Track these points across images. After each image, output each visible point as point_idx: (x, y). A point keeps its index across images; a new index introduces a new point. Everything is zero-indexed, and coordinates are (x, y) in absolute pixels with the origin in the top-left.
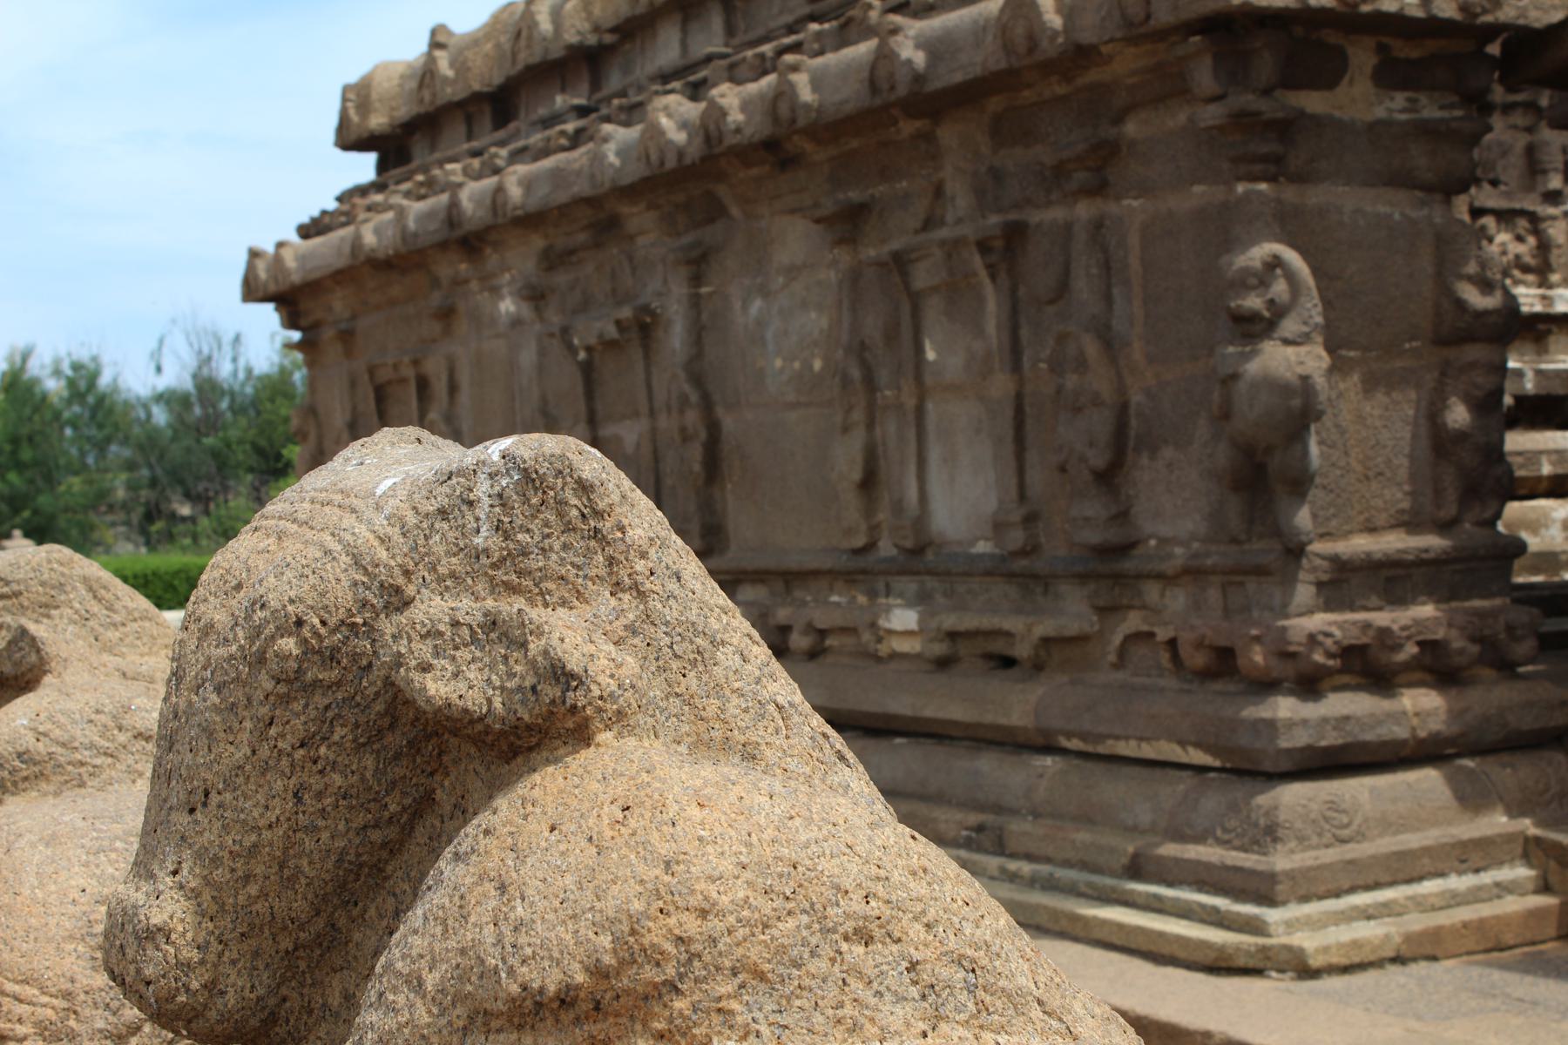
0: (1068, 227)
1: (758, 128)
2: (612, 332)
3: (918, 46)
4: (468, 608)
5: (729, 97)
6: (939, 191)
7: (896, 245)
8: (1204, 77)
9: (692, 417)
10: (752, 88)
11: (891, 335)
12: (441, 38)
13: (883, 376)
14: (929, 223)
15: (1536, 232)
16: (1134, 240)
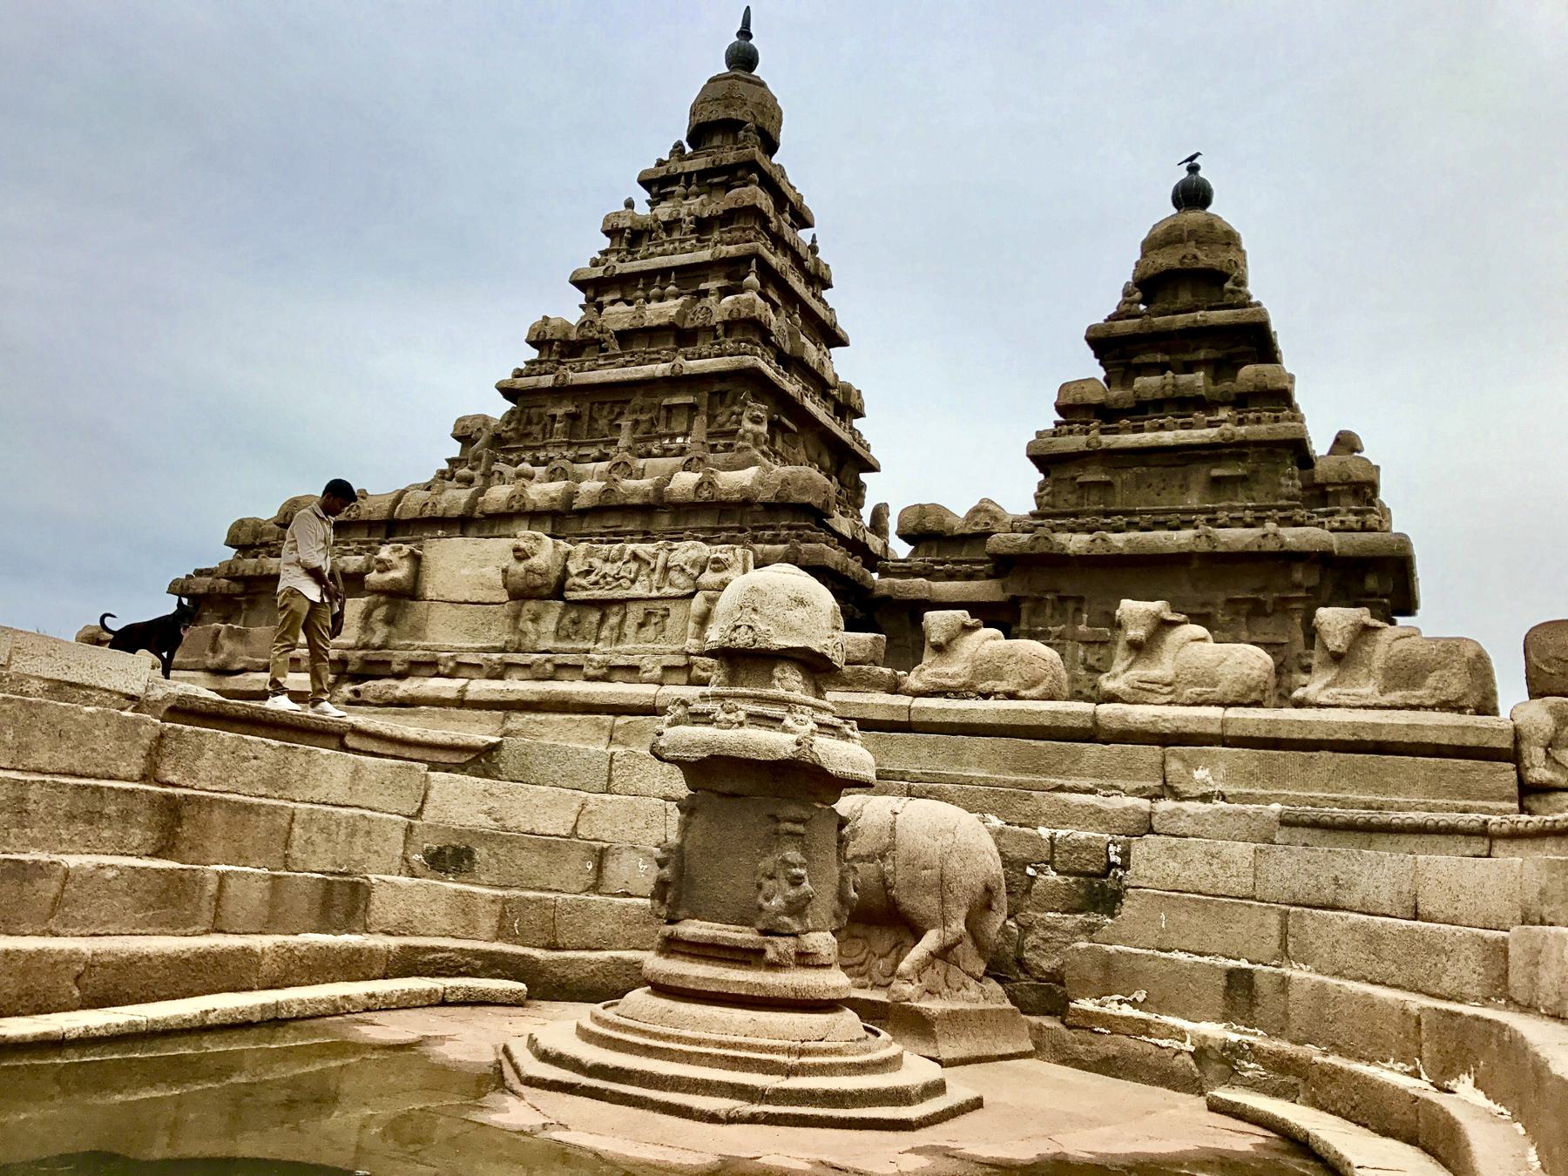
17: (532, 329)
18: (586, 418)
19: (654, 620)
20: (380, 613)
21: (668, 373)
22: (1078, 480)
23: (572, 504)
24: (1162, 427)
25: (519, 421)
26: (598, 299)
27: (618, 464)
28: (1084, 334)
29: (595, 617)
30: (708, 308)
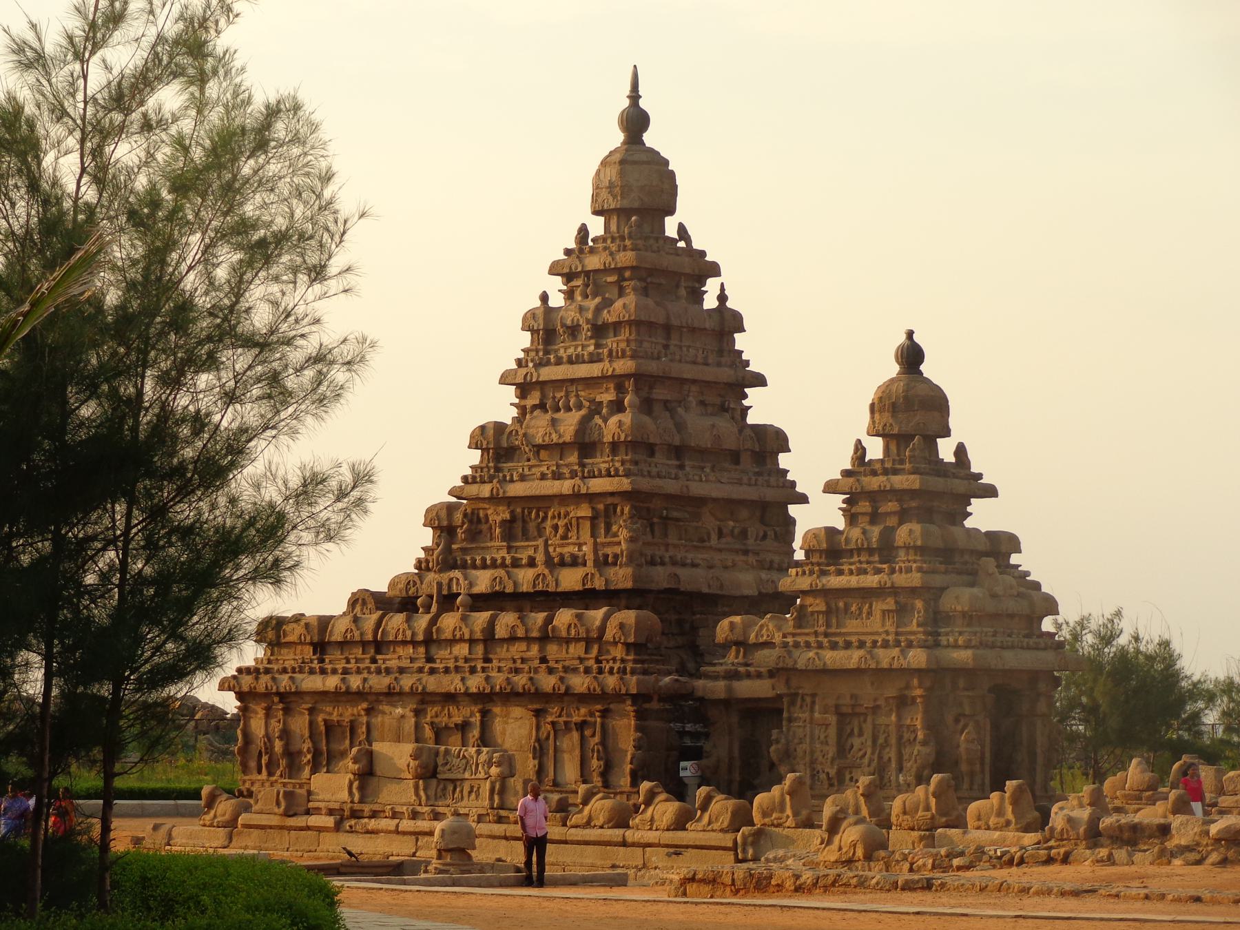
8: (629, 702)
17: (472, 437)
19: (475, 789)
20: (356, 784)
21: (571, 492)
22: (810, 609)
23: (494, 635)
24: (851, 572)
25: (471, 522)
26: (523, 403)
27: (539, 575)
29: (451, 788)
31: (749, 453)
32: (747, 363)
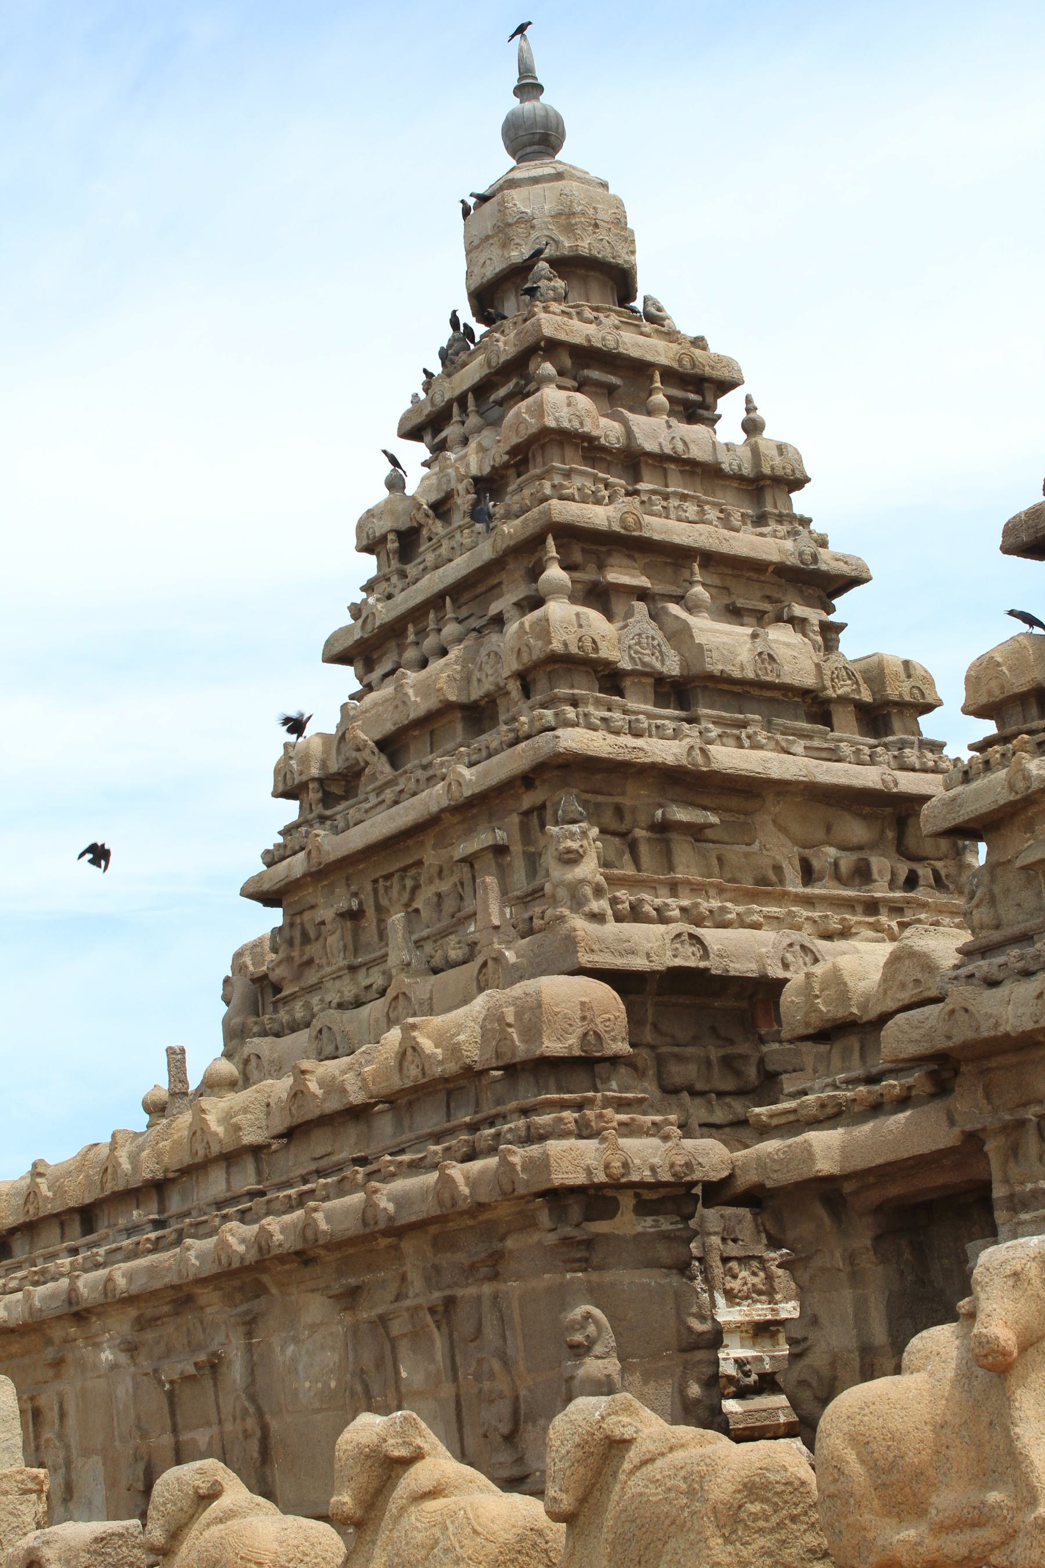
0: (479, 1298)
1: (293, 1244)
2: (191, 1370)
3: (389, 1200)
4: (400, 1441)
5: (274, 1224)
6: (403, 1278)
7: (380, 1310)
8: (544, 1218)
9: (251, 1423)
10: (287, 1218)
11: (379, 1364)
12: (40, 1170)
13: (375, 1389)
14: (398, 1298)
15: (764, 1269)
16: (515, 1305)
17: (277, 771)
18: (371, 913)
21: (445, 803)
22: (1019, 863)
25: (290, 943)
27: (396, 998)
28: (999, 540)
30: (496, 653)
31: (851, 708)
32: (822, 542)
